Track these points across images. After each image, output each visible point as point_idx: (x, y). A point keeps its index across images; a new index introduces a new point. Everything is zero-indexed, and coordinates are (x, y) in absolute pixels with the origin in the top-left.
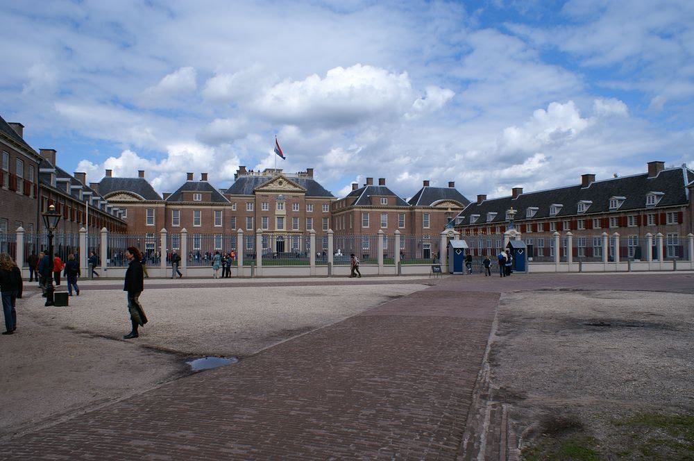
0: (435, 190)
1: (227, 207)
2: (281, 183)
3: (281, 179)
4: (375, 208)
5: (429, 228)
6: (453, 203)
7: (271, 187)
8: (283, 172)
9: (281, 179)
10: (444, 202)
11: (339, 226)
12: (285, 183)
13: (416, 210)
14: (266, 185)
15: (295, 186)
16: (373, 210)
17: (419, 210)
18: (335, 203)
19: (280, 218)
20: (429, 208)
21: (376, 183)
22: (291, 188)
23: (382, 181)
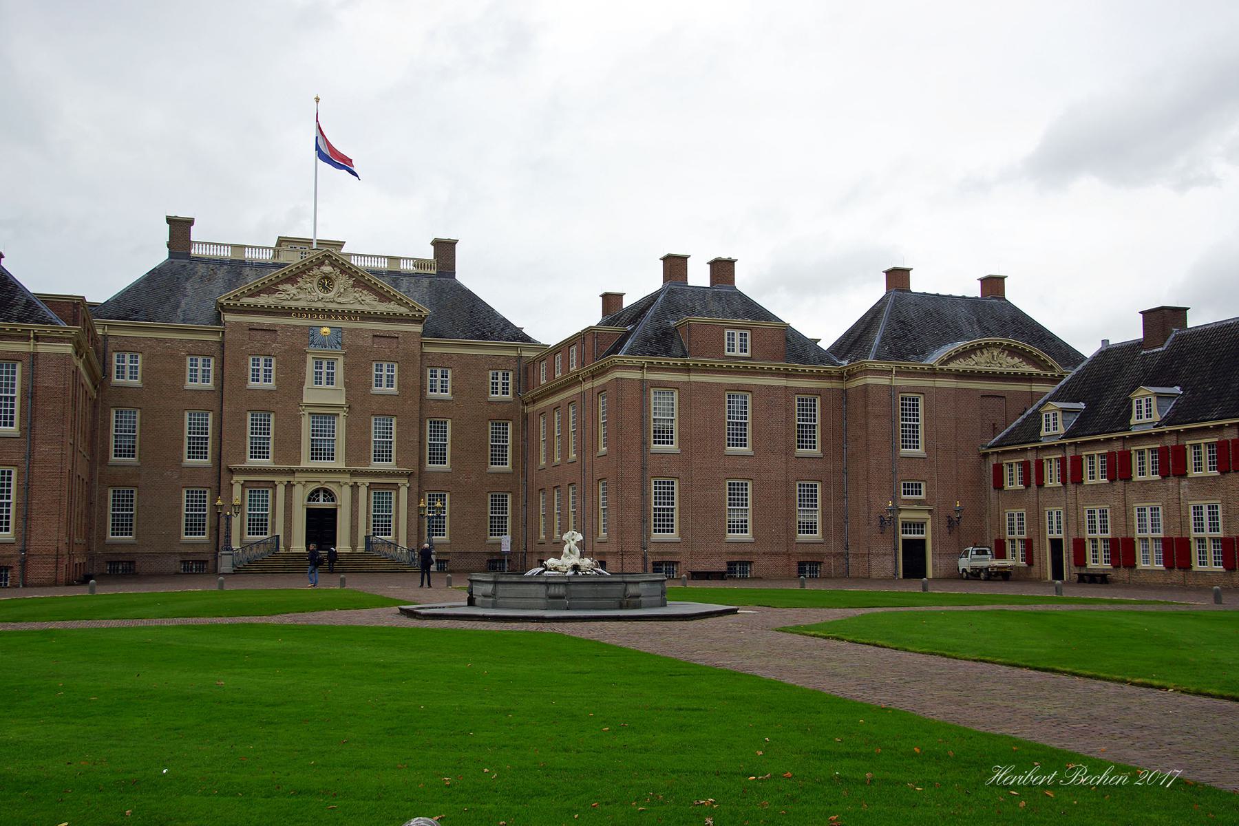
0: (937, 304)
1: (43, 348)
2: (326, 283)
3: (327, 269)
4: (705, 370)
5: (920, 451)
6: (1013, 351)
7: (289, 295)
8: (344, 250)
9: (327, 269)
10: (981, 348)
11: (550, 455)
12: (342, 282)
13: (871, 380)
14: (270, 289)
15: (383, 297)
16: (695, 378)
17: (883, 381)
18: (534, 362)
19: (324, 417)
20: (923, 373)
21: (698, 276)
22: (370, 303)
23: (722, 269)
